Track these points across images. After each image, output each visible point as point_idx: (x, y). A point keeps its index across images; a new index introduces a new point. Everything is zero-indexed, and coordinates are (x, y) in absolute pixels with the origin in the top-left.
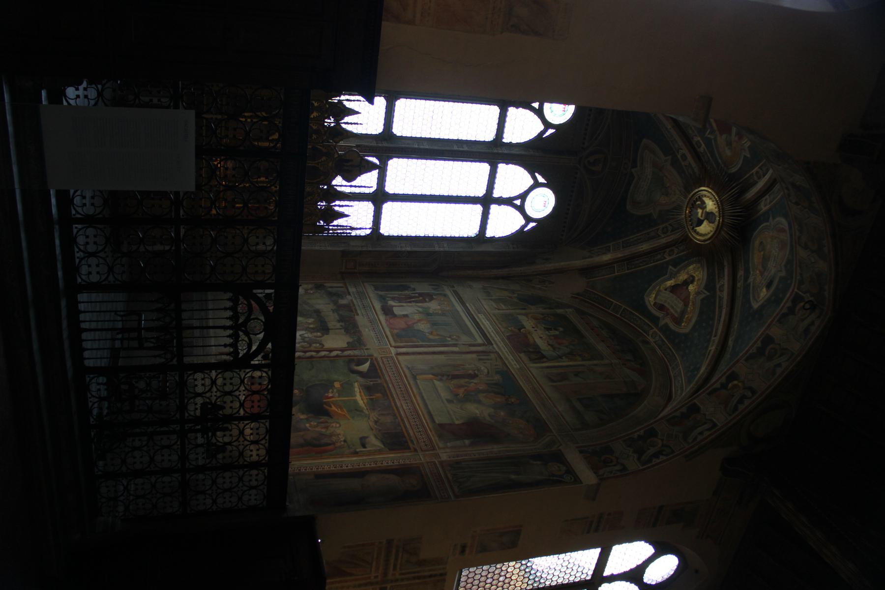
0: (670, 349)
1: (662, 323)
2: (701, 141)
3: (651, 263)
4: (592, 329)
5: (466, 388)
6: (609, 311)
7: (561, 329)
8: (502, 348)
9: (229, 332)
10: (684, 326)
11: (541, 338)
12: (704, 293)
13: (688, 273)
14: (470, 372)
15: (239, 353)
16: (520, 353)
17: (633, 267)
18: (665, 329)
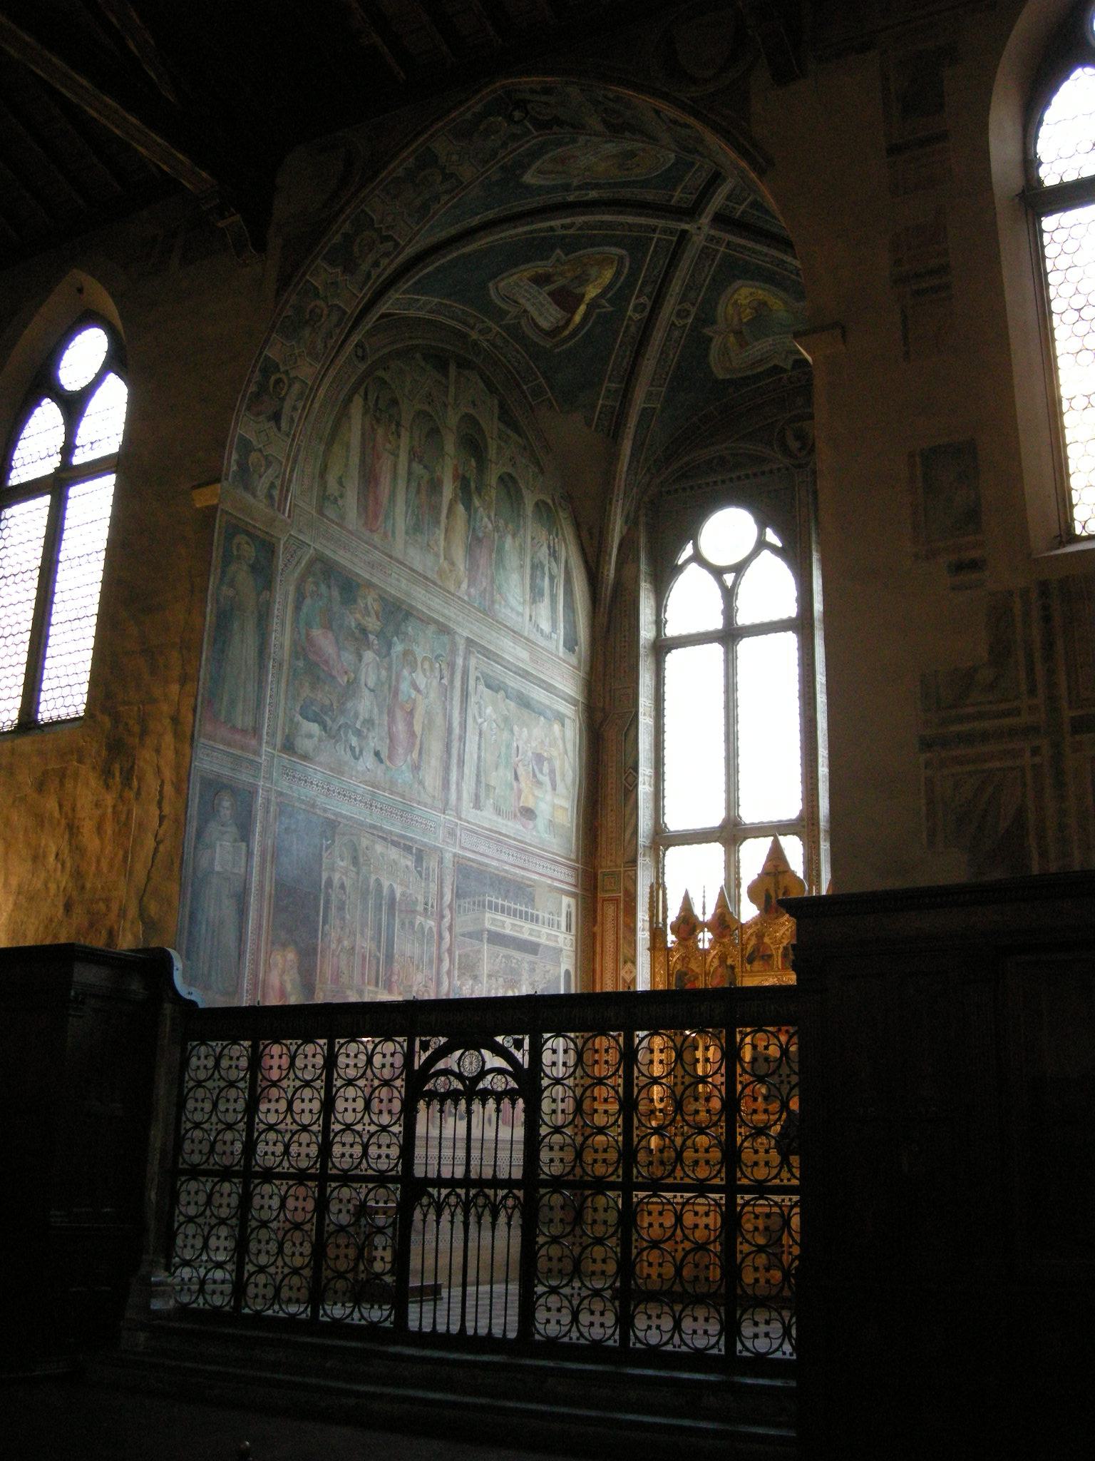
2: (631, 307)
9: (476, 1106)
15: (513, 1089)
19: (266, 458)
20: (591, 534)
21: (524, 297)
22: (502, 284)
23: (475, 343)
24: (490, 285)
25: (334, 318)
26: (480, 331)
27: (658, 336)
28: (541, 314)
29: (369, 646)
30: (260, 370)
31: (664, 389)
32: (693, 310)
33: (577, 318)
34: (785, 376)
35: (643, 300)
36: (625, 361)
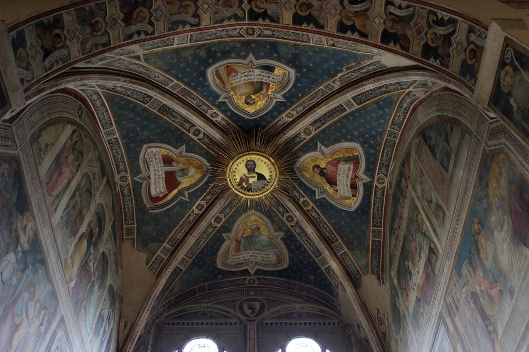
0: (382, 156)
1: (367, 179)
3: (322, 219)
4: (398, 237)
5: (489, 290)
6: (382, 240)
7: (406, 263)
8: (439, 299)
10: (356, 152)
11: (418, 272)
12: (320, 147)
13: (313, 177)
14: (472, 305)
16: (436, 274)
17: (333, 236)
18: (370, 171)
19: (28, 64)
20: (125, 326)
21: (154, 166)
22: (149, 150)
23: (115, 183)
24: (145, 146)
25: (104, 40)
26: (121, 177)
27: (203, 225)
28: (155, 184)
29: (15, 252)
30: (55, 16)
31: (190, 261)
32: (224, 220)
33: (169, 197)
34: (248, 278)
35: (203, 203)
36: (181, 234)
